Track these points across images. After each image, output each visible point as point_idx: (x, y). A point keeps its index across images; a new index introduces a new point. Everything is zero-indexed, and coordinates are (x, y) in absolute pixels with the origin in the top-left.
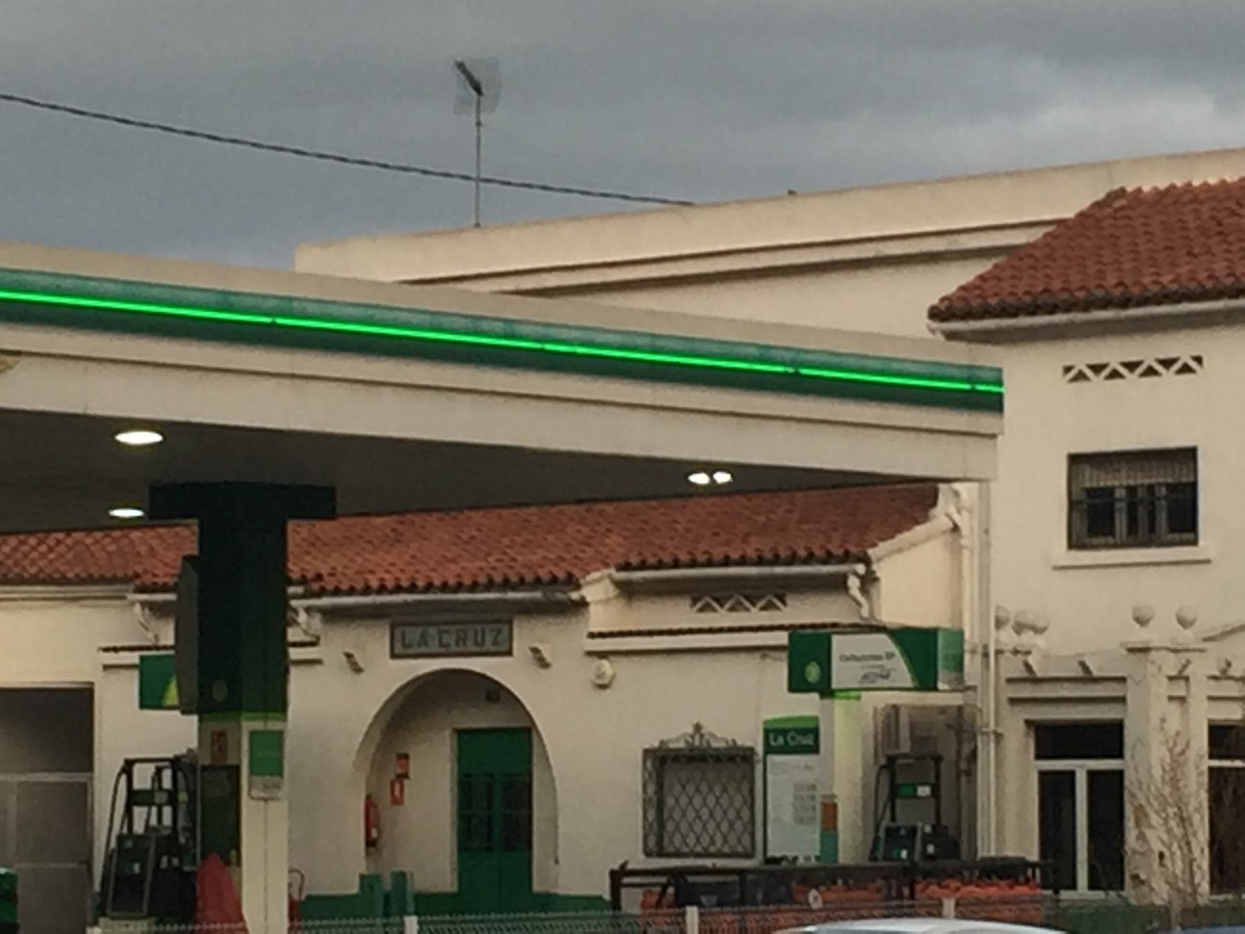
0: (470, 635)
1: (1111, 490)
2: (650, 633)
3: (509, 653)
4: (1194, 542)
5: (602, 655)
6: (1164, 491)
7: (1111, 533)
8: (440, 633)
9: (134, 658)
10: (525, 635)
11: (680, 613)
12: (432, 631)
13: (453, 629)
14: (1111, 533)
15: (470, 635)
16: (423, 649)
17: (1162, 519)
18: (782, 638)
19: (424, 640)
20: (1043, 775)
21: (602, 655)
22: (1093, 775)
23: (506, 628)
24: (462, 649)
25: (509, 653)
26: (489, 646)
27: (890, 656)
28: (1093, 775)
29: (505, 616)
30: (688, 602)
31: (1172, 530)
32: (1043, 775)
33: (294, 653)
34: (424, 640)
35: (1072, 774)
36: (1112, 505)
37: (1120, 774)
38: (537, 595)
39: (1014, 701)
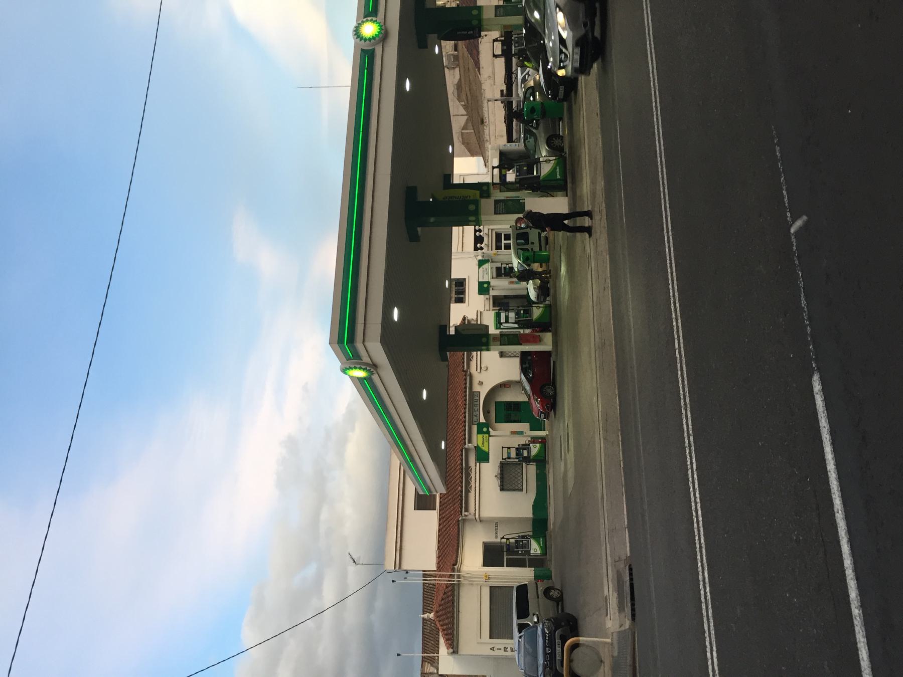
0: (475, 403)
1: (455, 298)
2: (477, 366)
3: (479, 392)
4: (465, 279)
5: (481, 368)
6: (456, 288)
7: (463, 282)
8: (475, 411)
9: (478, 464)
10: (476, 388)
11: (472, 495)
12: (474, 413)
13: (474, 408)
14: (462, 298)
15: (475, 403)
16: (478, 416)
17: (461, 288)
18: (478, 464)
19: (476, 416)
20: (505, 249)
21: (481, 368)
22: (505, 240)
23: (475, 393)
24: (478, 405)
25: (479, 392)
26: (478, 398)
27: (483, 268)
28: (505, 240)
29: (472, 393)
30: (471, 362)
31: (463, 286)
32: (505, 249)
33: (479, 323)
34: (476, 416)
35: (504, 243)
36: (458, 298)
37: (505, 235)
38: (468, 378)
39: (492, 250)
